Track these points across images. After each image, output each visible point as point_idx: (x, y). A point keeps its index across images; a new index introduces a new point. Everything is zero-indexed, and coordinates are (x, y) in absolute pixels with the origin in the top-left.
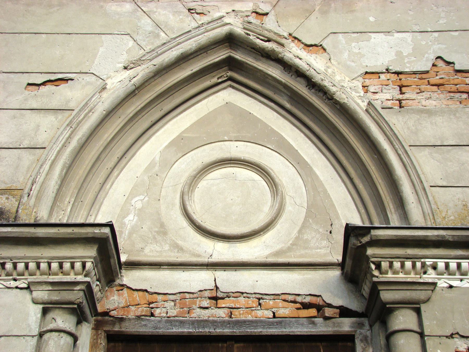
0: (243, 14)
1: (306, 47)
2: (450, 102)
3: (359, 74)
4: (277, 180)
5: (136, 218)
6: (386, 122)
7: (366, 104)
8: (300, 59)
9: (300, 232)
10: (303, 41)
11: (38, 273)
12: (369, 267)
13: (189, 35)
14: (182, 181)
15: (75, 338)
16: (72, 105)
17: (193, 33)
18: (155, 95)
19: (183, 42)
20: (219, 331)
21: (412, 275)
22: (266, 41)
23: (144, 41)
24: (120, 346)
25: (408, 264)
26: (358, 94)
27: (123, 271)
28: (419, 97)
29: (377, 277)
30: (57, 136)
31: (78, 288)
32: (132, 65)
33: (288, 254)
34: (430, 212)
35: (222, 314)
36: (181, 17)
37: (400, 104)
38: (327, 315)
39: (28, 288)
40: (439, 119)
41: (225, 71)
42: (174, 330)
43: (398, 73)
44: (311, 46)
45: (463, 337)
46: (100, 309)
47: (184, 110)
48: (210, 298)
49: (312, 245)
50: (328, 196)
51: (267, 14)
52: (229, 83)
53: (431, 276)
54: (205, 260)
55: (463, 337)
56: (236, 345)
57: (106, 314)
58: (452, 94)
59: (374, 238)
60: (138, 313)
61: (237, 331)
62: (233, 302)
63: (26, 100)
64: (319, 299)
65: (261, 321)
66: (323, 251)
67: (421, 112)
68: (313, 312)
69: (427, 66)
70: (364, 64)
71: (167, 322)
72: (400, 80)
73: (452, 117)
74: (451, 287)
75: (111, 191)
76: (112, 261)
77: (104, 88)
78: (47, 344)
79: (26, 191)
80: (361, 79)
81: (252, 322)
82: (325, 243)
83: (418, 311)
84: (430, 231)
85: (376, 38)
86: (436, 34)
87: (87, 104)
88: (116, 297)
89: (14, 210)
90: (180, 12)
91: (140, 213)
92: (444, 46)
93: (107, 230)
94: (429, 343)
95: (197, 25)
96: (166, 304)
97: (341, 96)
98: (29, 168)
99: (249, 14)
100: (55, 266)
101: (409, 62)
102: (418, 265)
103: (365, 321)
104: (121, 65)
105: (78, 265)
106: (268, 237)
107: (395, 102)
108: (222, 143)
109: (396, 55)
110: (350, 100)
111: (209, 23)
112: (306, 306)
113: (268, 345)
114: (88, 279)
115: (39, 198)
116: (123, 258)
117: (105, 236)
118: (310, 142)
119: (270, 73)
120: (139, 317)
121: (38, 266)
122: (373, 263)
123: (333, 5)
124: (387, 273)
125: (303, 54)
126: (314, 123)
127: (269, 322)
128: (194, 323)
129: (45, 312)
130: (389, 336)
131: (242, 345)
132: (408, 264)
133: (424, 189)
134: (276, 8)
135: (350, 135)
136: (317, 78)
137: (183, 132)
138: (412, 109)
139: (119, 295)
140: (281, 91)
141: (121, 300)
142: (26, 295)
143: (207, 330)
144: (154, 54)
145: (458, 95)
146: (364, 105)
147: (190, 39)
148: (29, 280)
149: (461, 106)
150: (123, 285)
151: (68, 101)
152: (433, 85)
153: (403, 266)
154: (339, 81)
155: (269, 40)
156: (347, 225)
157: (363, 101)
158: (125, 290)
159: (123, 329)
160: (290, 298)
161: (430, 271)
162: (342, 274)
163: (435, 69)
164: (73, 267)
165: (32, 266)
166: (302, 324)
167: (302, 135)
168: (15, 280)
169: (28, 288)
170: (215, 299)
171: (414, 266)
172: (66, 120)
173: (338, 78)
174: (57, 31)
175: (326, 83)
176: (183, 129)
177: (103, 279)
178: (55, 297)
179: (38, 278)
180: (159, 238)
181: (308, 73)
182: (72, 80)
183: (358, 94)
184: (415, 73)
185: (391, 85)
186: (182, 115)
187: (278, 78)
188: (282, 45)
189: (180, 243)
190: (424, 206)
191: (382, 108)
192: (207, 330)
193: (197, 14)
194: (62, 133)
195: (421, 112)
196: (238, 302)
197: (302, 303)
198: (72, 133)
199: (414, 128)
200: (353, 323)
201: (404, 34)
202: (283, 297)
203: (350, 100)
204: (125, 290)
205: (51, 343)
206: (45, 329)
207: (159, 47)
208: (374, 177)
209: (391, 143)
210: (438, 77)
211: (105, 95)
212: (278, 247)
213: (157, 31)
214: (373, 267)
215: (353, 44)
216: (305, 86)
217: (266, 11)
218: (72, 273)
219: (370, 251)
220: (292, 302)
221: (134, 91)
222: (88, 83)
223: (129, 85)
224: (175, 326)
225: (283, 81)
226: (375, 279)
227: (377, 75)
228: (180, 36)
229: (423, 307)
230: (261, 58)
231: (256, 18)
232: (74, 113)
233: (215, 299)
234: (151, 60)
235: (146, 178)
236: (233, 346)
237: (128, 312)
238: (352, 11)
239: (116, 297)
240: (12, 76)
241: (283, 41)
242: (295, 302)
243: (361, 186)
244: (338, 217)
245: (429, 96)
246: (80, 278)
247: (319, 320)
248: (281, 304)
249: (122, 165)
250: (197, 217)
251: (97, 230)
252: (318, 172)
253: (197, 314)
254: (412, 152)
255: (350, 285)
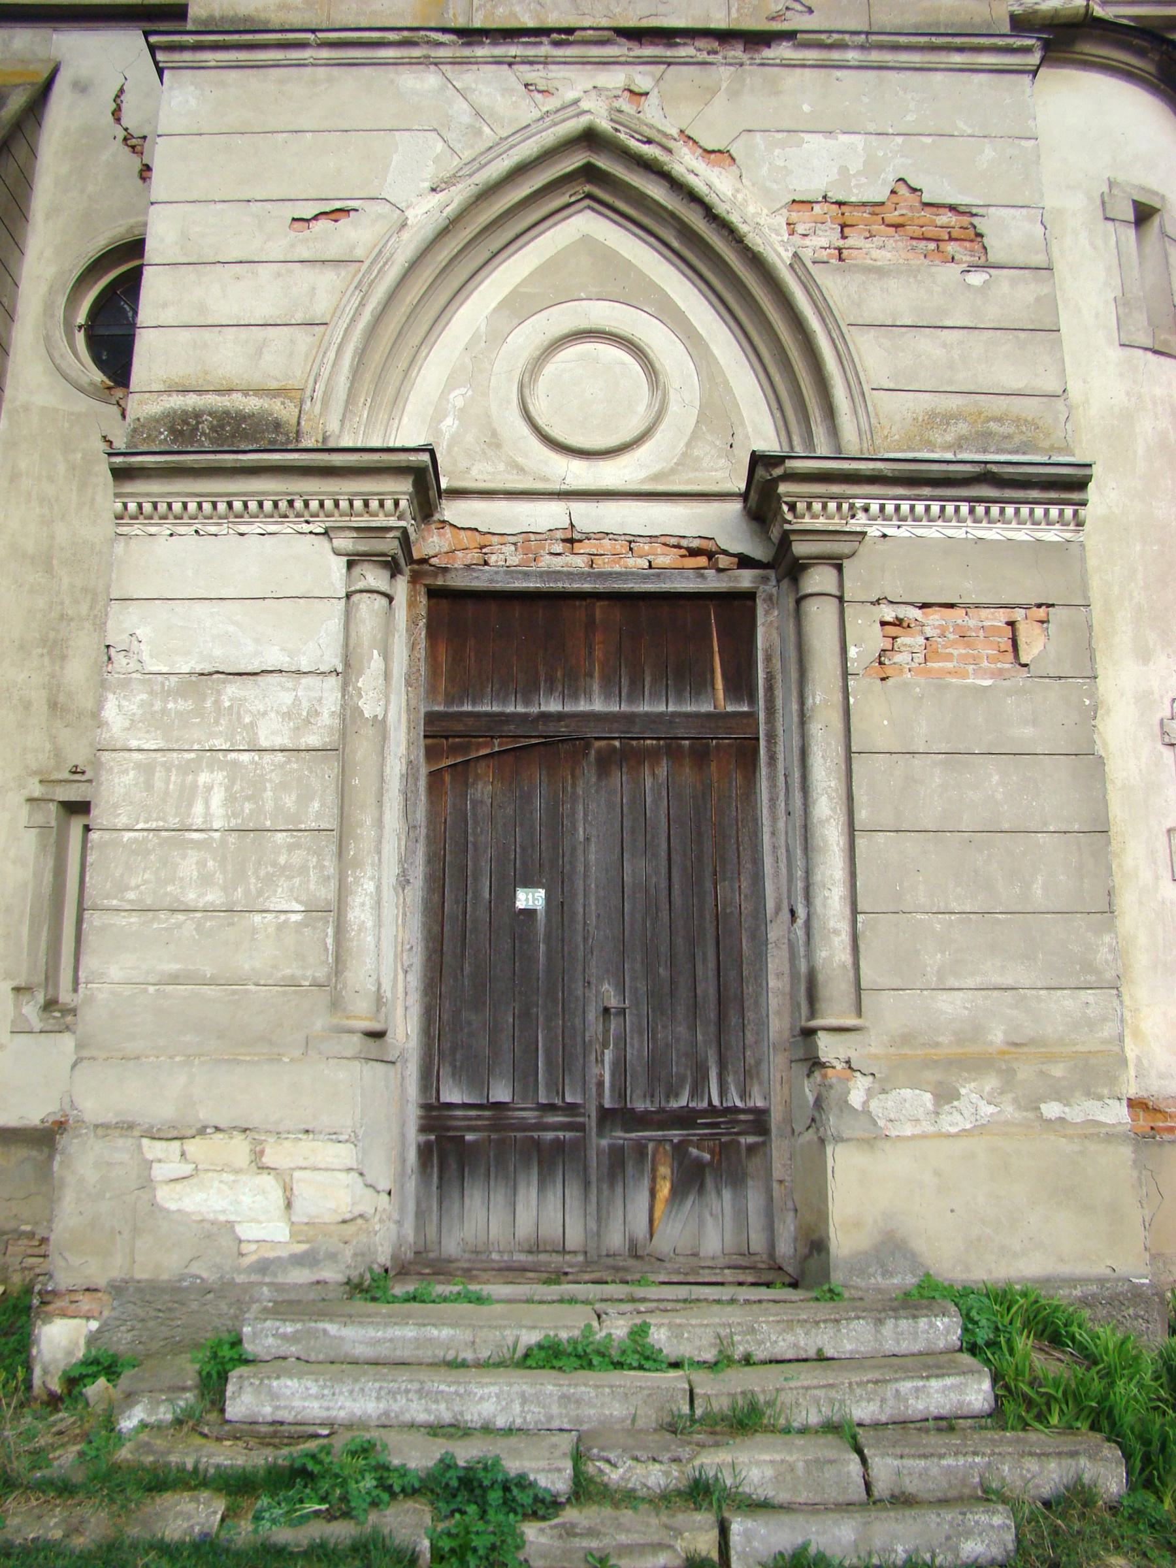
0: (609, 93)
1: (705, 154)
2: (911, 255)
3: (783, 203)
4: (657, 366)
5: (457, 422)
6: (818, 286)
7: (790, 254)
8: (696, 175)
9: (688, 445)
10: (701, 144)
11: (336, 513)
12: (780, 508)
13: (527, 133)
14: (520, 365)
15: (390, 599)
16: (359, 253)
17: (533, 129)
18: (478, 230)
19: (519, 143)
20: (576, 586)
21: (836, 521)
22: (644, 143)
23: (460, 141)
24: (445, 604)
25: (832, 506)
26: (780, 238)
27: (444, 502)
28: (867, 244)
29: (789, 522)
30: (342, 305)
31: (391, 535)
32: (443, 186)
33: (671, 478)
34: (867, 428)
35: (579, 562)
36: (514, 99)
37: (840, 254)
38: (721, 566)
39: (326, 533)
40: (892, 283)
41: (581, 184)
42: (516, 585)
43: (840, 204)
44: (713, 152)
45: (892, 602)
46: (416, 556)
47: (520, 248)
48: (564, 541)
49: (705, 465)
50: (729, 390)
51: (647, 94)
52: (587, 202)
53: (859, 522)
54: (556, 486)
55: (892, 602)
56: (598, 604)
57: (424, 561)
58: (914, 243)
59: (788, 471)
60: (468, 562)
61: (600, 587)
62: (595, 546)
63: (293, 246)
64: (711, 542)
65: (632, 574)
66: (719, 475)
67: (869, 270)
68: (702, 561)
69: (882, 194)
70: (791, 187)
71: (507, 573)
72: (843, 214)
73: (911, 280)
74: (885, 536)
75: (419, 379)
76: (431, 493)
77: (404, 225)
78: (358, 609)
79: (308, 393)
80: (784, 211)
81: (620, 574)
82: (722, 462)
83: (839, 568)
84: (863, 462)
85: (814, 142)
86: (899, 140)
87: (380, 252)
88: (435, 539)
89: (295, 421)
90: (512, 90)
91: (462, 413)
92: (910, 161)
93: (425, 457)
94: (849, 610)
95: (539, 115)
96: (505, 549)
97: (755, 241)
98: (307, 356)
99: (620, 93)
100: (358, 504)
101: (857, 186)
102: (845, 506)
103: (771, 573)
104: (427, 185)
105: (389, 504)
106: (642, 452)
107: (833, 251)
108: (576, 303)
109: (839, 173)
110: (768, 248)
111: (558, 111)
112: (693, 552)
113: (641, 603)
114: (403, 523)
115: (325, 403)
116: (443, 486)
117: (422, 465)
118: (706, 303)
119: (649, 193)
120: (468, 566)
121: (337, 505)
122: (786, 503)
123: (748, 81)
124: (803, 517)
125: (699, 165)
126: (713, 273)
127: (643, 575)
128: (541, 575)
129: (350, 565)
130: (799, 601)
131: (606, 603)
132: (832, 506)
133: (863, 394)
134: (661, 82)
135: (766, 300)
136: (721, 209)
137: (519, 285)
138: (855, 265)
139: (440, 535)
140: (664, 219)
141: (442, 543)
142: (323, 542)
143: (559, 586)
144: (476, 165)
145: (923, 244)
146: (787, 256)
147: (529, 138)
148: (328, 524)
149: (927, 262)
150: (444, 522)
151: (353, 248)
152: (888, 226)
153: (824, 507)
154: (753, 215)
155: (649, 142)
156: (753, 453)
157: (787, 250)
158: (447, 527)
159: (448, 583)
160: (673, 541)
161: (861, 514)
162: (745, 507)
163: (894, 198)
164: (382, 505)
165: (329, 504)
166: (688, 578)
167: (696, 291)
168: (308, 522)
169: (326, 533)
170: (571, 541)
171: (839, 507)
172: (352, 279)
173: (751, 209)
174: (326, 126)
175: (735, 219)
176: (518, 280)
177: (418, 518)
178: (363, 547)
179: (337, 520)
180: (490, 453)
181: (707, 199)
182: (357, 210)
183: (780, 238)
184: (864, 204)
185: (829, 224)
186: (516, 256)
187: (662, 201)
188: (669, 151)
189: (520, 460)
190: (861, 420)
191: (814, 263)
192: (560, 585)
193: (539, 92)
194: (349, 301)
195: (869, 270)
196: (602, 546)
197: (687, 549)
198: (363, 299)
199: (856, 297)
200: (756, 577)
201: (853, 136)
202: (663, 539)
203: (768, 248)
204: (447, 527)
205: (363, 606)
206: (353, 589)
207: (482, 153)
208: (796, 368)
209: (823, 320)
210: (896, 213)
211: (406, 235)
212: (656, 468)
213: (479, 123)
214: (785, 508)
215: (777, 151)
216: (701, 217)
217: (644, 89)
218: (381, 514)
219: (783, 488)
220: (674, 546)
221: (447, 227)
222: (380, 216)
223: (440, 220)
224: (518, 579)
225: (670, 207)
226: (787, 527)
227: (809, 206)
228: (513, 134)
229: (846, 563)
230: (636, 167)
231: (630, 102)
232: (364, 267)
233: (571, 541)
234: (470, 175)
235: (467, 360)
236: (594, 604)
237: (454, 559)
238: (777, 93)
239: (435, 539)
240: (268, 206)
241: (671, 144)
242: (678, 547)
243: (777, 378)
244: (743, 424)
245: (881, 244)
246: (393, 522)
247: (711, 573)
248: (660, 549)
249: (433, 340)
250: (541, 422)
251: (412, 457)
252: (716, 352)
253: (547, 562)
254: (853, 335)
255: (755, 525)
